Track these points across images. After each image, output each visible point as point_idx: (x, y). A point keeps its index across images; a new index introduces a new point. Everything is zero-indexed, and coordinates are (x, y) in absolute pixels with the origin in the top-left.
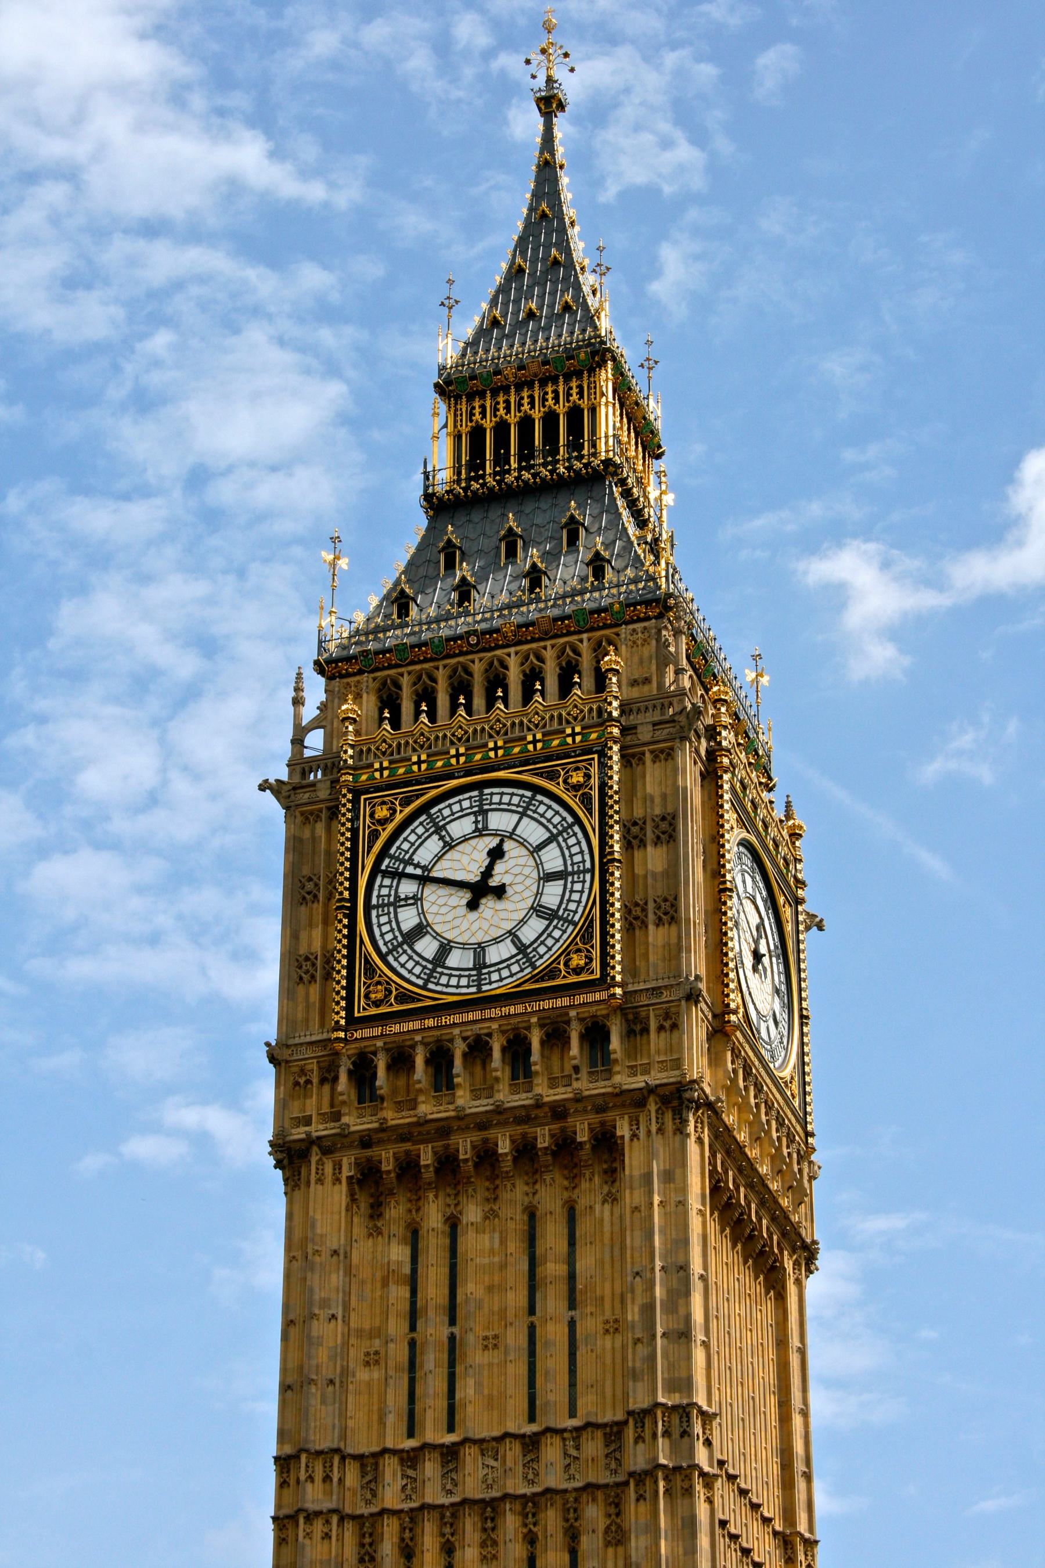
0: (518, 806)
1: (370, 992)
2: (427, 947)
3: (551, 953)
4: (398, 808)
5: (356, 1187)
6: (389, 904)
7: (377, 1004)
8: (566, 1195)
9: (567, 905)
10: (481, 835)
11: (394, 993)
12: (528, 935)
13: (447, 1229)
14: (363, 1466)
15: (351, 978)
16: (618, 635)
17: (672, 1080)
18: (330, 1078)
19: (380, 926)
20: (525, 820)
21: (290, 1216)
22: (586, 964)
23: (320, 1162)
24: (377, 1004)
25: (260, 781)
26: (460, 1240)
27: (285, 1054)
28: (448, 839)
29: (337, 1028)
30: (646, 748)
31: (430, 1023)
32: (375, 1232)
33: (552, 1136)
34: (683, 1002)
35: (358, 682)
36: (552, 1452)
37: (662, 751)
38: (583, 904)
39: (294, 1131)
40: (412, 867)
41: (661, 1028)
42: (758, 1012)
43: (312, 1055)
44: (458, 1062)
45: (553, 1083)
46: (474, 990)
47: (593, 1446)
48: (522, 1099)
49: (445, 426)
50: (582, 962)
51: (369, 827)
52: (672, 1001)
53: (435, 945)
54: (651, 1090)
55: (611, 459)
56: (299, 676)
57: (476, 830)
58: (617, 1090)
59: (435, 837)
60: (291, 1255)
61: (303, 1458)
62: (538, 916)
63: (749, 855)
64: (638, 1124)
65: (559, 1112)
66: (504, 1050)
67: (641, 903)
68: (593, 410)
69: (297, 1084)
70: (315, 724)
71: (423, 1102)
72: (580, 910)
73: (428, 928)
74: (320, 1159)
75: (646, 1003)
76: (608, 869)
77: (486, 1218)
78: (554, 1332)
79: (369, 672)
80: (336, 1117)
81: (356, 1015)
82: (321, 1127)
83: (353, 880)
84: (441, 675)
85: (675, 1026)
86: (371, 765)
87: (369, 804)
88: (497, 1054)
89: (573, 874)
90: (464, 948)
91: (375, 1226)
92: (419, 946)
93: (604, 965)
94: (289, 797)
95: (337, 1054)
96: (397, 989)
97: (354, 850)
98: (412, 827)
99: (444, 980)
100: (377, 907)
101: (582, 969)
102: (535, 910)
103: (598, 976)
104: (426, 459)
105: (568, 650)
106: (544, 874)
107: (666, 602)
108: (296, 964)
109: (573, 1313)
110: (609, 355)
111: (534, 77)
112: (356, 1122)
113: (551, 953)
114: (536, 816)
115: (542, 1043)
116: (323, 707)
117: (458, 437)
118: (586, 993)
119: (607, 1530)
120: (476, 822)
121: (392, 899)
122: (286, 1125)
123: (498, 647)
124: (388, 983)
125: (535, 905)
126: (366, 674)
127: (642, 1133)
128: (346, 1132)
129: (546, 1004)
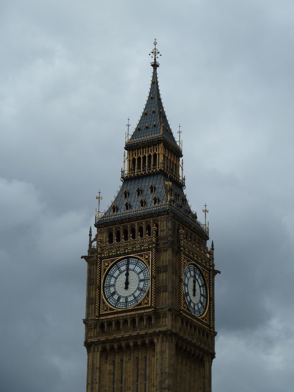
2: (116, 297)
3: (141, 299)
4: (110, 263)
7: (105, 311)
12: (136, 294)
15: (100, 305)
17: (165, 330)
22: (148, 302)
28: (120, 271)
31: (116, 316)
37: (165, 249)
40: (113, 277)
41: (163, 317)
46: (125, 308)
48: (135, 334)
49: (127, 158)
50: (147, 302)
52: (166, 311)
53: (117, 296)
54: (160, 332)
58: (154, 332)
64: (158, 339)
65: (142, 336)
66: (131, 322)
68: (159, 154)
69: (89, 329)
70: (95, 240)
71: (114, 334)
81: (101, 313)
83: (100, 281)
85: (166, 317)
86: (104, 253)
88: (129, 323)
89: (146, 280)
91: (106, 361)
92: (114, 297)
94: (88, 259)
97: (100, 273)
98: (113, 268)
100: (106, 287)
101: (147, 303)
102: (138, 289)
103: (150, 305)
109: (146, 382)
113: (141, 299)
115: (139, 321)
116: (97, 236)
117: (129, 161)
120: (126, 267)
123: (133, 221)
126: (105, 227)
129: (139, 312)
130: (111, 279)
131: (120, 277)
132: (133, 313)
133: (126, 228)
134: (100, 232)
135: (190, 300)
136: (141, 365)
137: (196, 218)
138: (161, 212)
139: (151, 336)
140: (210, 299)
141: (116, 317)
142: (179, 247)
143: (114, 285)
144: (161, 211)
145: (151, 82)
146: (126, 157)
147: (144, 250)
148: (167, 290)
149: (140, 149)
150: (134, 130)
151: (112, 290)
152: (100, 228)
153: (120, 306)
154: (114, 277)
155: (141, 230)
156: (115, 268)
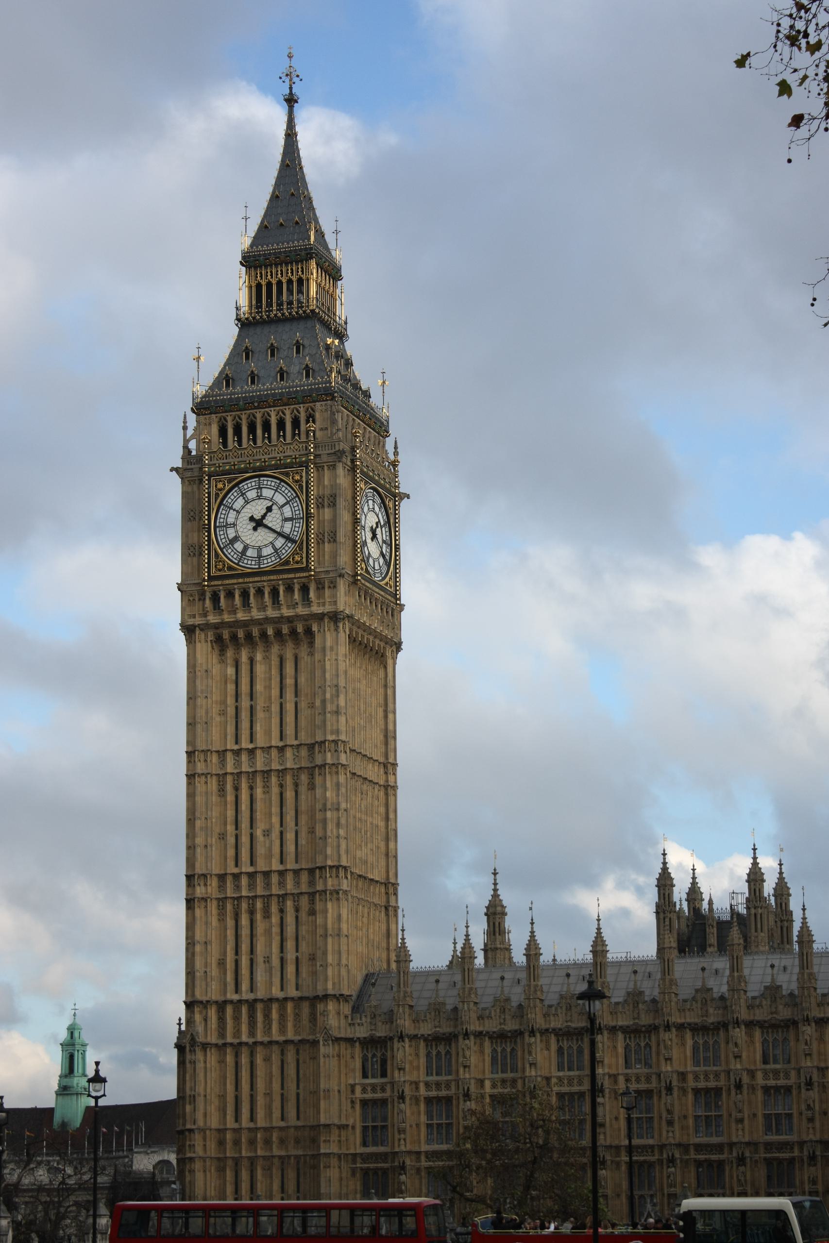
2: (239, 546)
6: (224, 526)
7: (220, 570)
10: (259, 499)
14: (219, 755)
20: (277, 493)
24: (220, 570)
27: (184, 588)
31: (240, 580)
32: (222, 661)
36: (289, 753)
46: (257, 567)
47: (304, 752)
49: (245, 282)
56: (185, 415)
57: (258, 496)
59: (241, 498)
61: (196, 752)
65: (290, 620)
68: (308, 280)
69: (189, 600)
70: (192, 437)
78: (290, 707)
80: (205, 615)
83: (209, 515)
84: (244, 417)
85: (335, 587)
89: (295, 519)
93: (307, 561)
99: (246, 561)
105: (295, 411)
112: (213, 619)
116: (195, 429)
117: (250, 287)
119: (309, 784)
120: (258, 492)
129: (285, 576)
131: (245, 510)
135: (369, 553)
136: (289, 669)
137: (370, 397)
138: (322, 395)
139: (306, 620)
140: (396, 548)
141: (240, 583)
142: (353, 461)
143: (234, 525)
146: (242, 281)
147: (290, 466)
150: (256, 228)
151: (231, 533)
152: (203, 415)
153: (247, 564)
154: (234, 510)
155: (281, 425)
156: (235, 493)
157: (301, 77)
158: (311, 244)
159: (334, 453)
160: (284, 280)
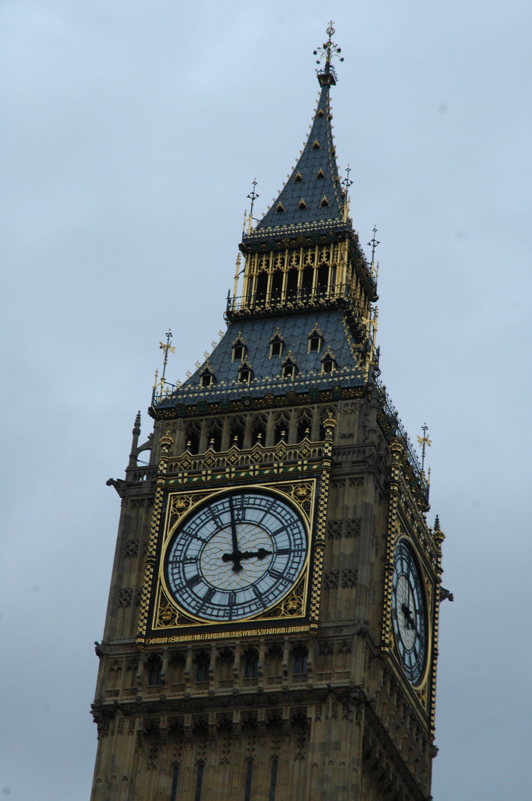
0: (265, 507)
1: (163, 615)
2: (201, 590)
4: (191, 502)
5: (143, 737)
6: (180, 562)
7: (166, 623)
8: (272, 752)
9: (289, 570)
11: (177, 617)
12: (263, 587)
13: (197, 769)
16: (336, 406)
17: (344, 685)
18: (133, 667)
19: (173, 574)
20: (268, 516)
21: (99, 753)
22: (298, 608)
23: (121, 720)
25: (108, 479)
26: (205, 776)
27: (107, 650)
28: (220, 524)
29: (140, 636)
30: (347, 477)
31: (198, 637)
33: (266, 714)
34: (355, 637)
35: (175, 423)
37: (356, 479)
38: (299, 570)
39: (107, 699)
40: (196, 540)
41: (340, 651)
42: (404, 648)
43: (123, 652)
44: (213, 663)
45: (271, 681)
49: (244, 271)
50: (295, 607)
51: (172, 513)
53: (206, 589)
54: (330, 690)
55: (342, 299)
56: (138, 417)
58: (310, 689)
59: (212, 522)
60: (98, 778)
62: (271, 576)
63: (407, 550)
64: (320, 711)
66: (242, 658)
67: (335, 572)
68: (334, 267)
71: (189, 687)
72: (297, 574)
73: (203, 578)
74: (122, 718)
75: (332, 635)
76: (316, 550)
77: (222, 763)
79: (181, 418)
80: (134, 692)
81: (153, 629)
82: (124, 698)
84: (226, 423)
85: (349, 651)
87: (174, 498)
88: (237, 660)
89: (294, 551)
90: (223, 592)
91: (152, 763)
92: (196, 589)
93: (308, 609)
94: (125, 490)
95: (139, 652)
96: (179, 615)
97: (161, 526)
98: (198, 515)
99: (209, 611)
100: (172, 563)
103: (304, 616)
104: (229, 290)
106: (277, 550)
107: (368, 388)
108: (119, 594)
110: (347, 235)
111: (318, 62)
113: (277, 599)
114: (275, 513)
115: (266, 655)
116: (152, 437)
117: (251, 278)
118: (296, 626)
121: (182, 558)
122: (103, 695)
124: (174, 611)
125: (269, 569)
126: (180, 419)
127: (323, 717)
128: (140, 702)
129: (271, 631)
130: (191, 544)
131: (215, 539)
132: (249, 633)
133: (239, 423)
134: (162, 428)
138: (348, 388)
141: (197, 641)
143: (196, 560)
144: (347, 386)
145: (314, 114)
146: (242, 267)
147: (295, 475)
148: (354, 583)
149: (283, 252)
151: (191, 571)
152: (165, 419)
157: (342, 55)
158: (343, 223)
159: (364, 461)
160: (300, 267)
